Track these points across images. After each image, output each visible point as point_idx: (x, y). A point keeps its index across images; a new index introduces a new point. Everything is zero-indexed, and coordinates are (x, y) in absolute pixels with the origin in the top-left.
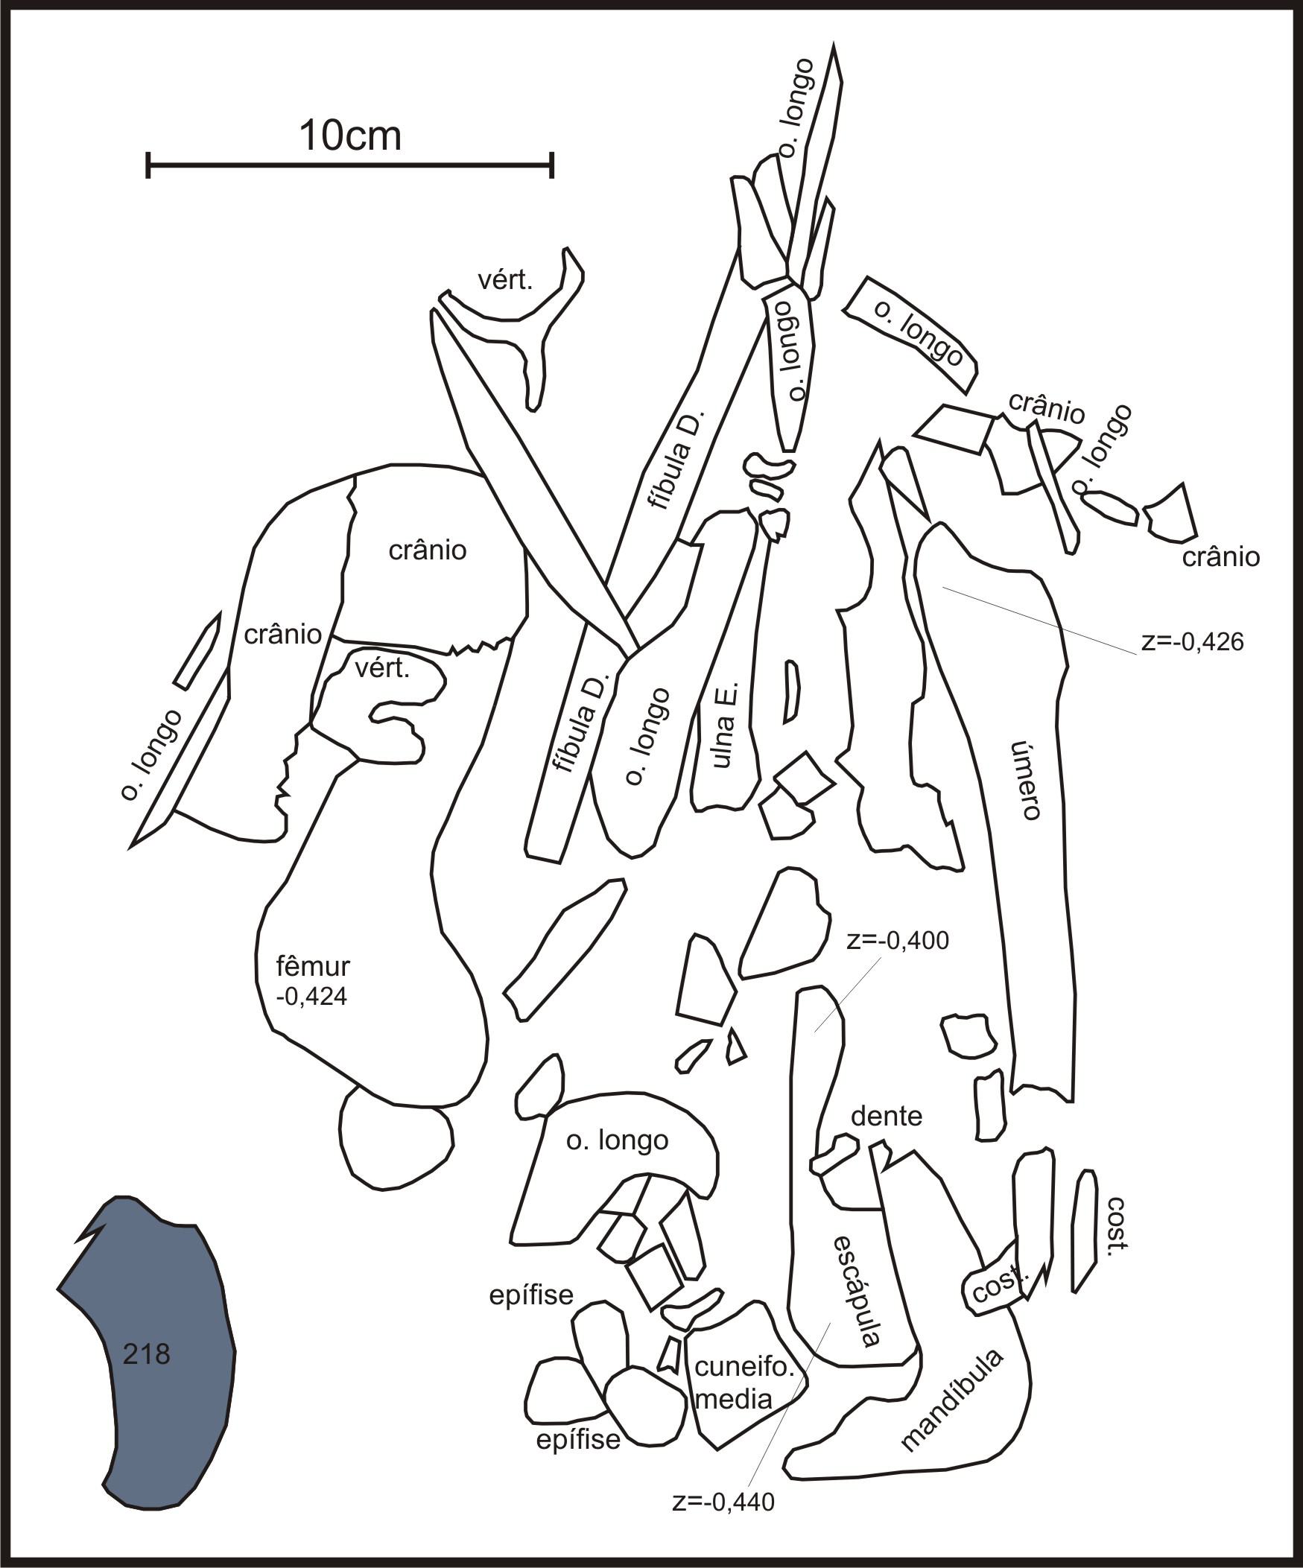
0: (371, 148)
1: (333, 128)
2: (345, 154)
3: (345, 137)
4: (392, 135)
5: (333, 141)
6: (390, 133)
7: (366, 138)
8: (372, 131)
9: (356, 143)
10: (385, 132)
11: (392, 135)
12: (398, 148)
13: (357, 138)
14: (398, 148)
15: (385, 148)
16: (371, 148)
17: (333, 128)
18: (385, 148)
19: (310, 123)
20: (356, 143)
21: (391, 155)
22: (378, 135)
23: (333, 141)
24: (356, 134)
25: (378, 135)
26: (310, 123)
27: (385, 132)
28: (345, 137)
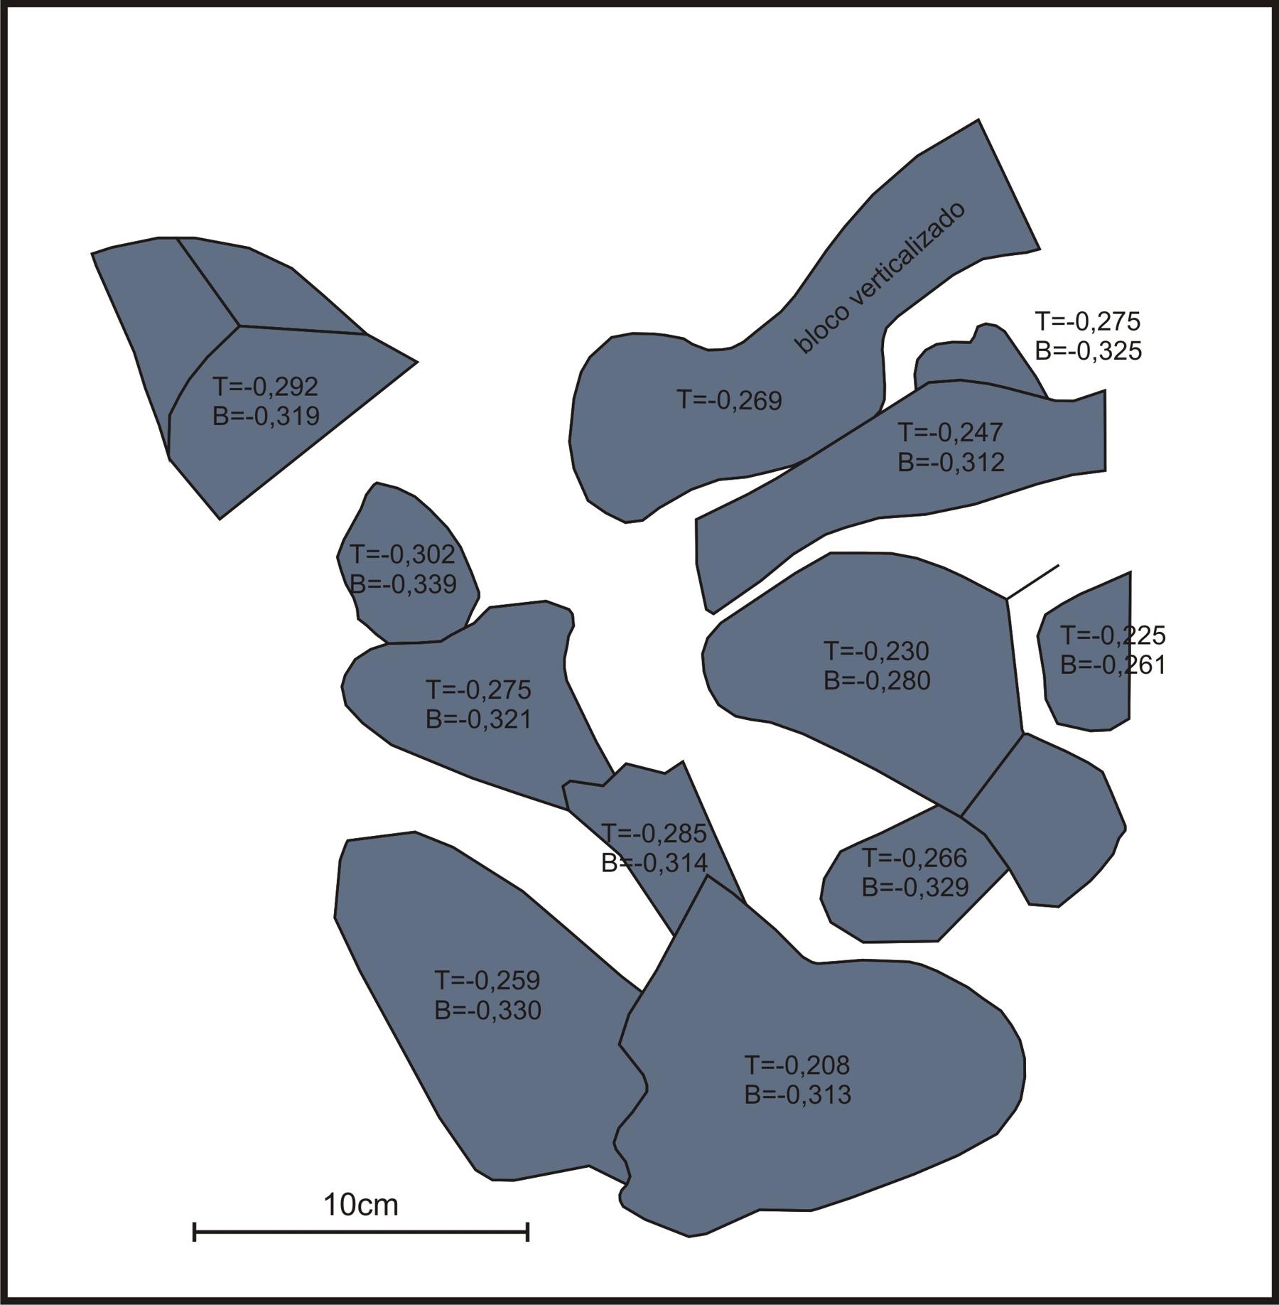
1: (348, 1199)
3: (357, 1206)
4: (391, 1204)
5: (348, 1209)
6: (390, 1204)
7: (372, 1207)
8: (377, 1202)
9: (365, 1210)
10: (386, 1202)
11: (391, 1204)
13: (366, 1207)
17: (348, 1198)
19: (331, 1196)
20: (365, 1210)
22: (381, 1204)
23: (348, 1209)
25: (381, 1204)
26: (331, 1196)
27: (386, 1202)
28: (357, 1206)
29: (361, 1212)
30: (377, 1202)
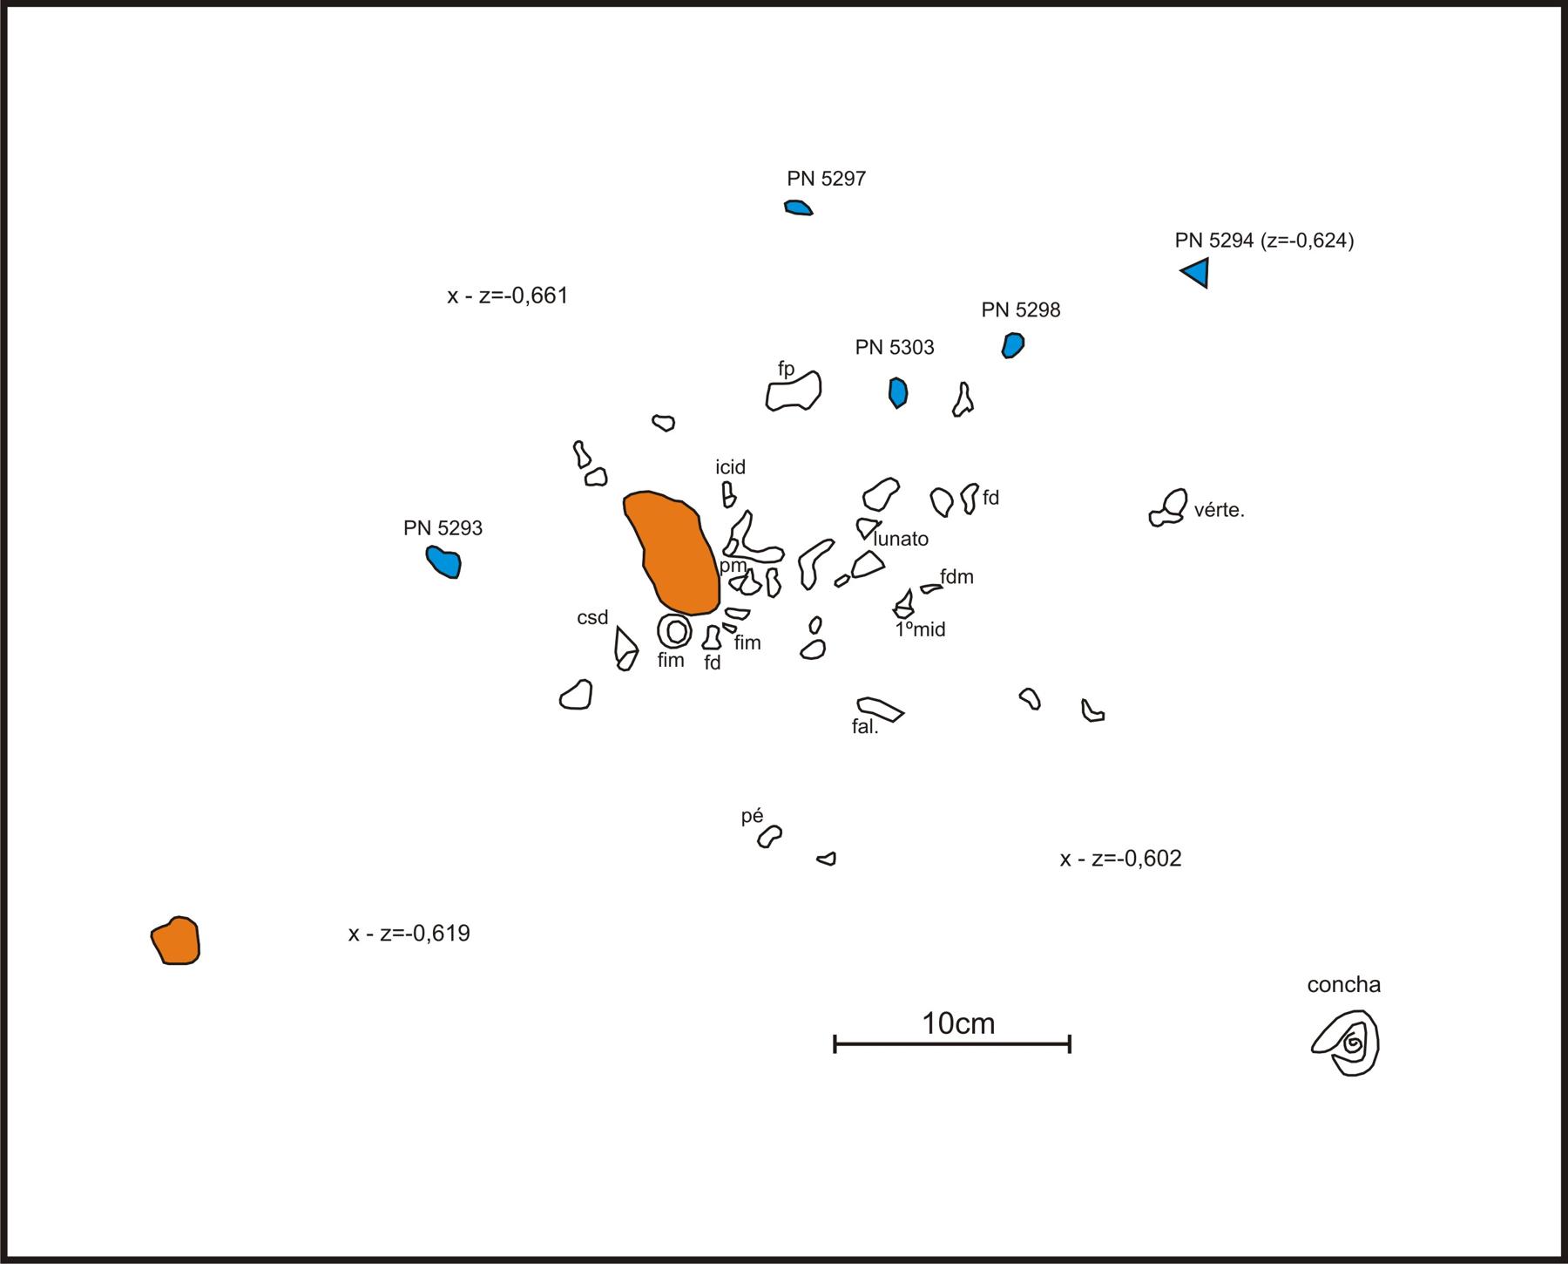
1: (946, 1017)
2: (955, 1037)
3: (955, 1025)
4: (988, 1023)
5: (946, 1029)
6: (987, 1022)
7: (970, 1025)
9: (963, 1029)
11: (988, 1023)
13: (964, 1026)
17: (946, 1017)
19: (930, 1015)
20: (963, 1029)
21: (987, 1037)
22: (978, 1023)
23: (946, 1029)
25: (978, 1023)
26: (930, 1015)
28: (955, 1025)
29: (958, 1031)
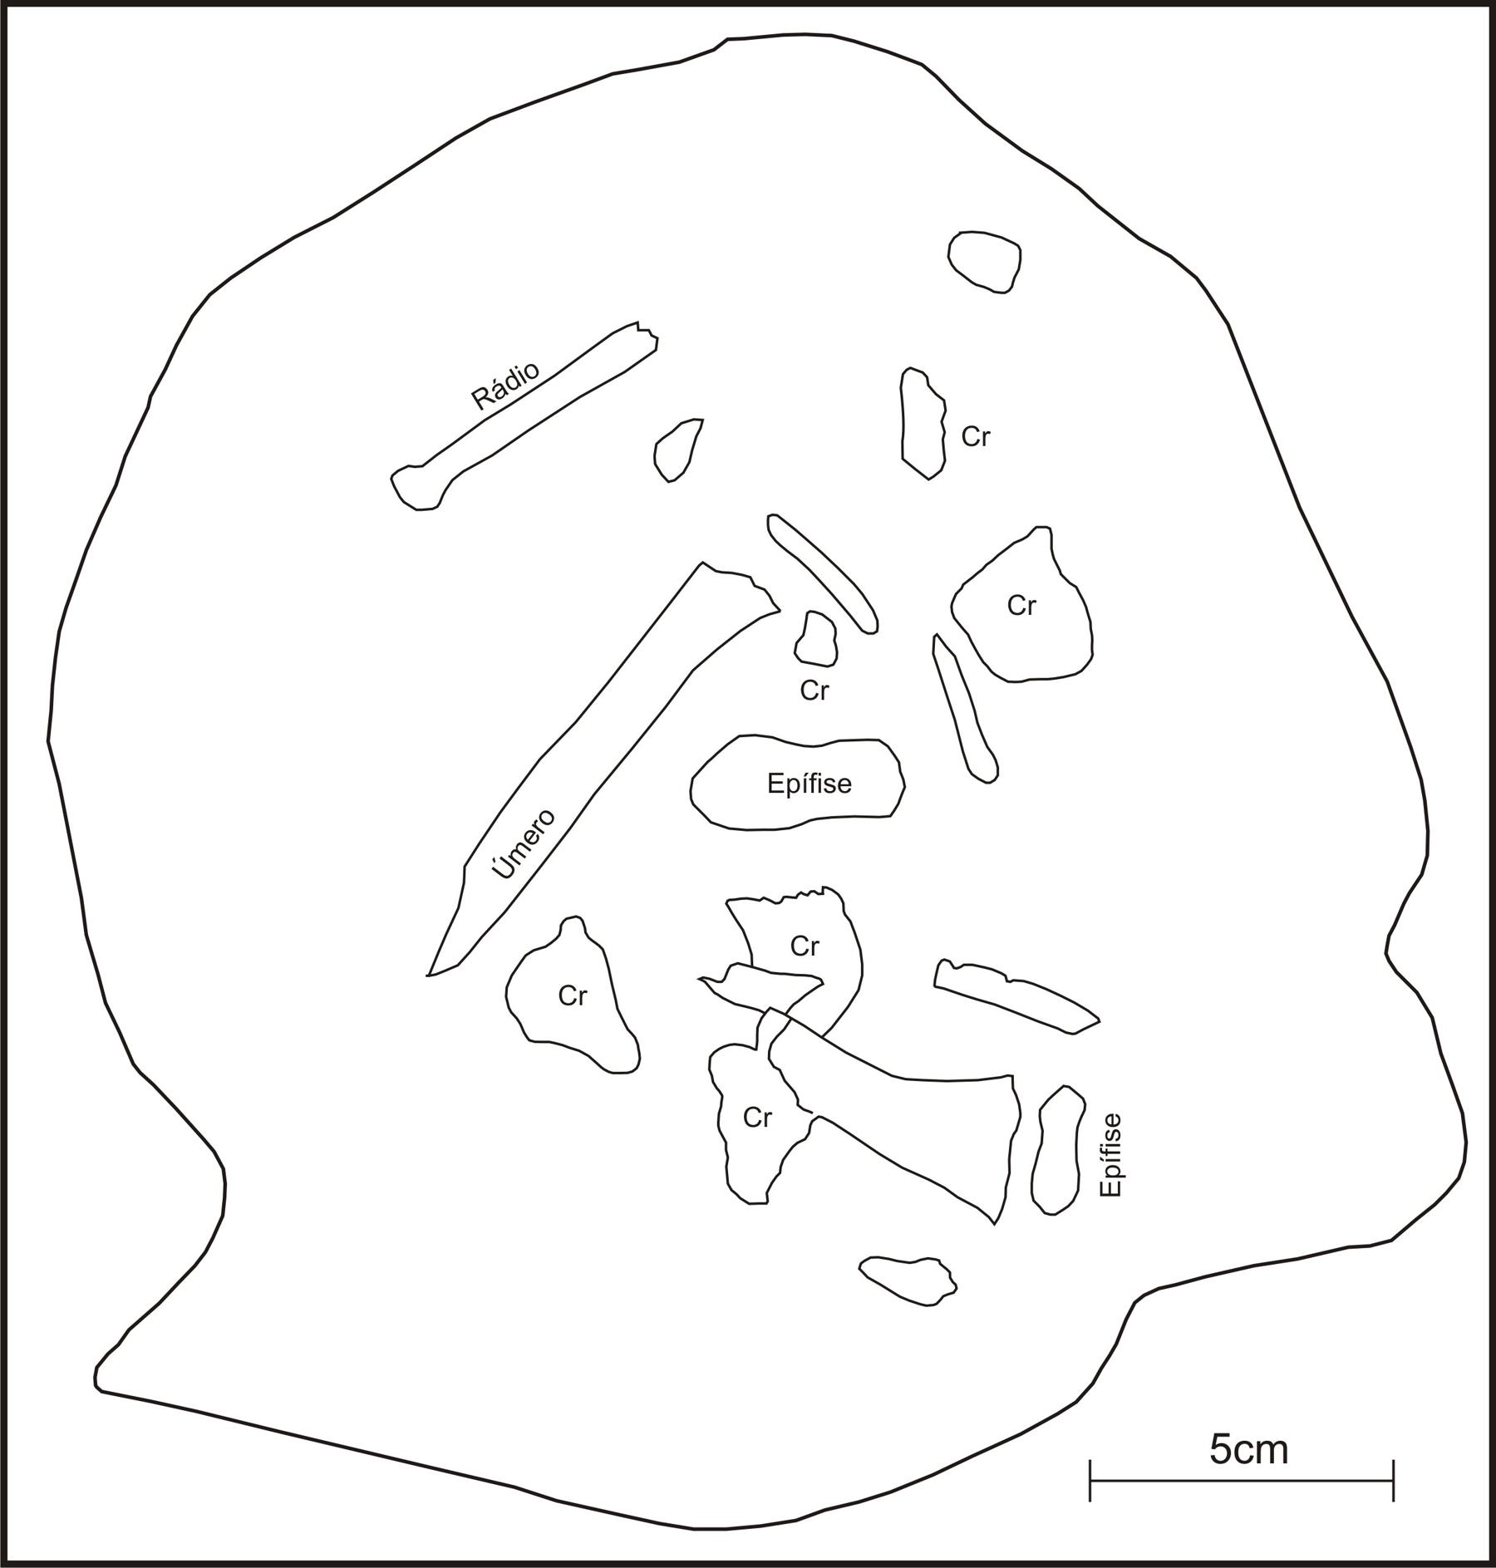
0: (1259, 1461)
4: (1279, 1449)
6: (1276, 1448)
7: (1254, 1452)
8: (1260, 1445)
9: (1244, 1456)
10: (1272, 1446)
11: (1279, 1449)
12: (1285, 1461)
13: (1245, 1452)
14: (1285, 1461)
15: (1272, 1461)
16: (1259, 1461)
18: (1272, 1461)
20: (1244, 1456)
22: (1266, 1449)
24: (1244, 1447)
25: (1266, 1449)
27: (1272, 1446)
28: (1233, 1453)
30: (1260, 1445)
